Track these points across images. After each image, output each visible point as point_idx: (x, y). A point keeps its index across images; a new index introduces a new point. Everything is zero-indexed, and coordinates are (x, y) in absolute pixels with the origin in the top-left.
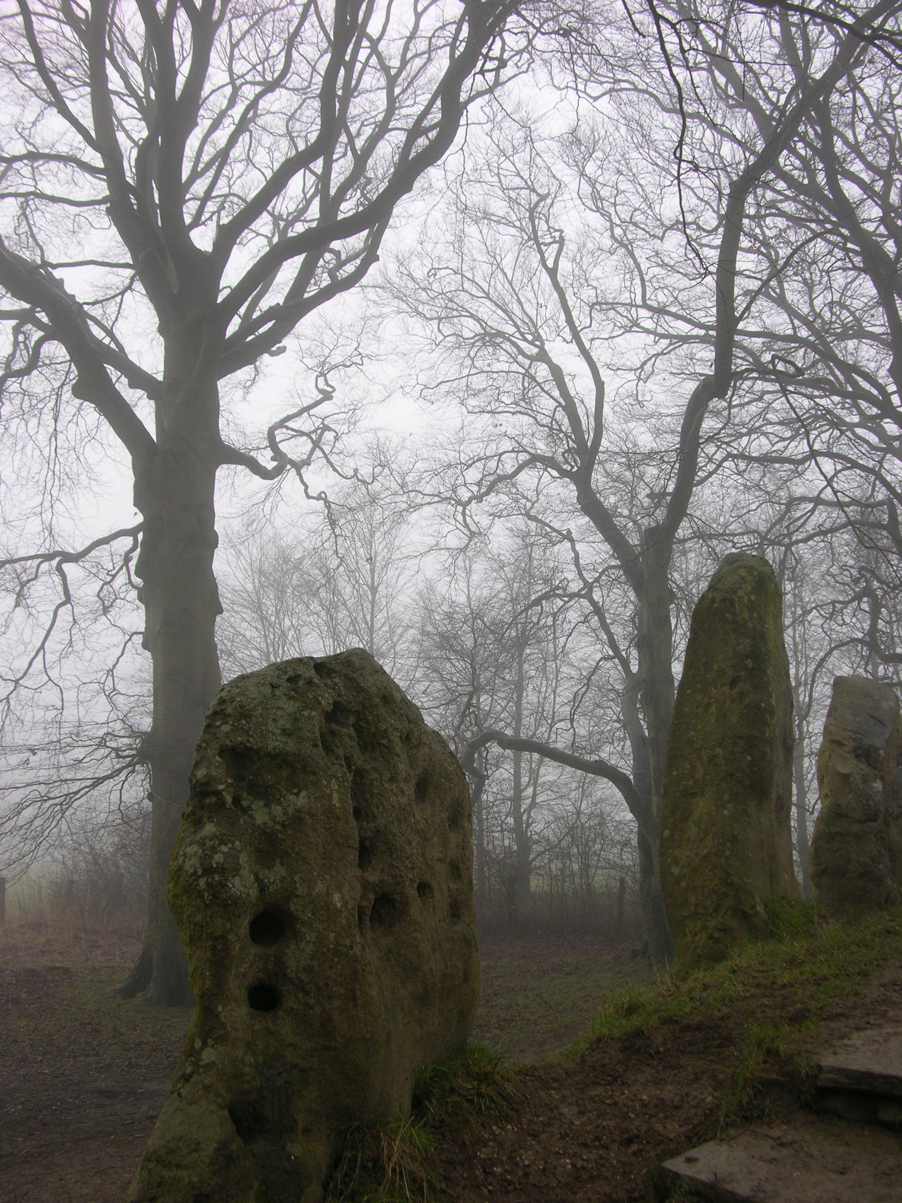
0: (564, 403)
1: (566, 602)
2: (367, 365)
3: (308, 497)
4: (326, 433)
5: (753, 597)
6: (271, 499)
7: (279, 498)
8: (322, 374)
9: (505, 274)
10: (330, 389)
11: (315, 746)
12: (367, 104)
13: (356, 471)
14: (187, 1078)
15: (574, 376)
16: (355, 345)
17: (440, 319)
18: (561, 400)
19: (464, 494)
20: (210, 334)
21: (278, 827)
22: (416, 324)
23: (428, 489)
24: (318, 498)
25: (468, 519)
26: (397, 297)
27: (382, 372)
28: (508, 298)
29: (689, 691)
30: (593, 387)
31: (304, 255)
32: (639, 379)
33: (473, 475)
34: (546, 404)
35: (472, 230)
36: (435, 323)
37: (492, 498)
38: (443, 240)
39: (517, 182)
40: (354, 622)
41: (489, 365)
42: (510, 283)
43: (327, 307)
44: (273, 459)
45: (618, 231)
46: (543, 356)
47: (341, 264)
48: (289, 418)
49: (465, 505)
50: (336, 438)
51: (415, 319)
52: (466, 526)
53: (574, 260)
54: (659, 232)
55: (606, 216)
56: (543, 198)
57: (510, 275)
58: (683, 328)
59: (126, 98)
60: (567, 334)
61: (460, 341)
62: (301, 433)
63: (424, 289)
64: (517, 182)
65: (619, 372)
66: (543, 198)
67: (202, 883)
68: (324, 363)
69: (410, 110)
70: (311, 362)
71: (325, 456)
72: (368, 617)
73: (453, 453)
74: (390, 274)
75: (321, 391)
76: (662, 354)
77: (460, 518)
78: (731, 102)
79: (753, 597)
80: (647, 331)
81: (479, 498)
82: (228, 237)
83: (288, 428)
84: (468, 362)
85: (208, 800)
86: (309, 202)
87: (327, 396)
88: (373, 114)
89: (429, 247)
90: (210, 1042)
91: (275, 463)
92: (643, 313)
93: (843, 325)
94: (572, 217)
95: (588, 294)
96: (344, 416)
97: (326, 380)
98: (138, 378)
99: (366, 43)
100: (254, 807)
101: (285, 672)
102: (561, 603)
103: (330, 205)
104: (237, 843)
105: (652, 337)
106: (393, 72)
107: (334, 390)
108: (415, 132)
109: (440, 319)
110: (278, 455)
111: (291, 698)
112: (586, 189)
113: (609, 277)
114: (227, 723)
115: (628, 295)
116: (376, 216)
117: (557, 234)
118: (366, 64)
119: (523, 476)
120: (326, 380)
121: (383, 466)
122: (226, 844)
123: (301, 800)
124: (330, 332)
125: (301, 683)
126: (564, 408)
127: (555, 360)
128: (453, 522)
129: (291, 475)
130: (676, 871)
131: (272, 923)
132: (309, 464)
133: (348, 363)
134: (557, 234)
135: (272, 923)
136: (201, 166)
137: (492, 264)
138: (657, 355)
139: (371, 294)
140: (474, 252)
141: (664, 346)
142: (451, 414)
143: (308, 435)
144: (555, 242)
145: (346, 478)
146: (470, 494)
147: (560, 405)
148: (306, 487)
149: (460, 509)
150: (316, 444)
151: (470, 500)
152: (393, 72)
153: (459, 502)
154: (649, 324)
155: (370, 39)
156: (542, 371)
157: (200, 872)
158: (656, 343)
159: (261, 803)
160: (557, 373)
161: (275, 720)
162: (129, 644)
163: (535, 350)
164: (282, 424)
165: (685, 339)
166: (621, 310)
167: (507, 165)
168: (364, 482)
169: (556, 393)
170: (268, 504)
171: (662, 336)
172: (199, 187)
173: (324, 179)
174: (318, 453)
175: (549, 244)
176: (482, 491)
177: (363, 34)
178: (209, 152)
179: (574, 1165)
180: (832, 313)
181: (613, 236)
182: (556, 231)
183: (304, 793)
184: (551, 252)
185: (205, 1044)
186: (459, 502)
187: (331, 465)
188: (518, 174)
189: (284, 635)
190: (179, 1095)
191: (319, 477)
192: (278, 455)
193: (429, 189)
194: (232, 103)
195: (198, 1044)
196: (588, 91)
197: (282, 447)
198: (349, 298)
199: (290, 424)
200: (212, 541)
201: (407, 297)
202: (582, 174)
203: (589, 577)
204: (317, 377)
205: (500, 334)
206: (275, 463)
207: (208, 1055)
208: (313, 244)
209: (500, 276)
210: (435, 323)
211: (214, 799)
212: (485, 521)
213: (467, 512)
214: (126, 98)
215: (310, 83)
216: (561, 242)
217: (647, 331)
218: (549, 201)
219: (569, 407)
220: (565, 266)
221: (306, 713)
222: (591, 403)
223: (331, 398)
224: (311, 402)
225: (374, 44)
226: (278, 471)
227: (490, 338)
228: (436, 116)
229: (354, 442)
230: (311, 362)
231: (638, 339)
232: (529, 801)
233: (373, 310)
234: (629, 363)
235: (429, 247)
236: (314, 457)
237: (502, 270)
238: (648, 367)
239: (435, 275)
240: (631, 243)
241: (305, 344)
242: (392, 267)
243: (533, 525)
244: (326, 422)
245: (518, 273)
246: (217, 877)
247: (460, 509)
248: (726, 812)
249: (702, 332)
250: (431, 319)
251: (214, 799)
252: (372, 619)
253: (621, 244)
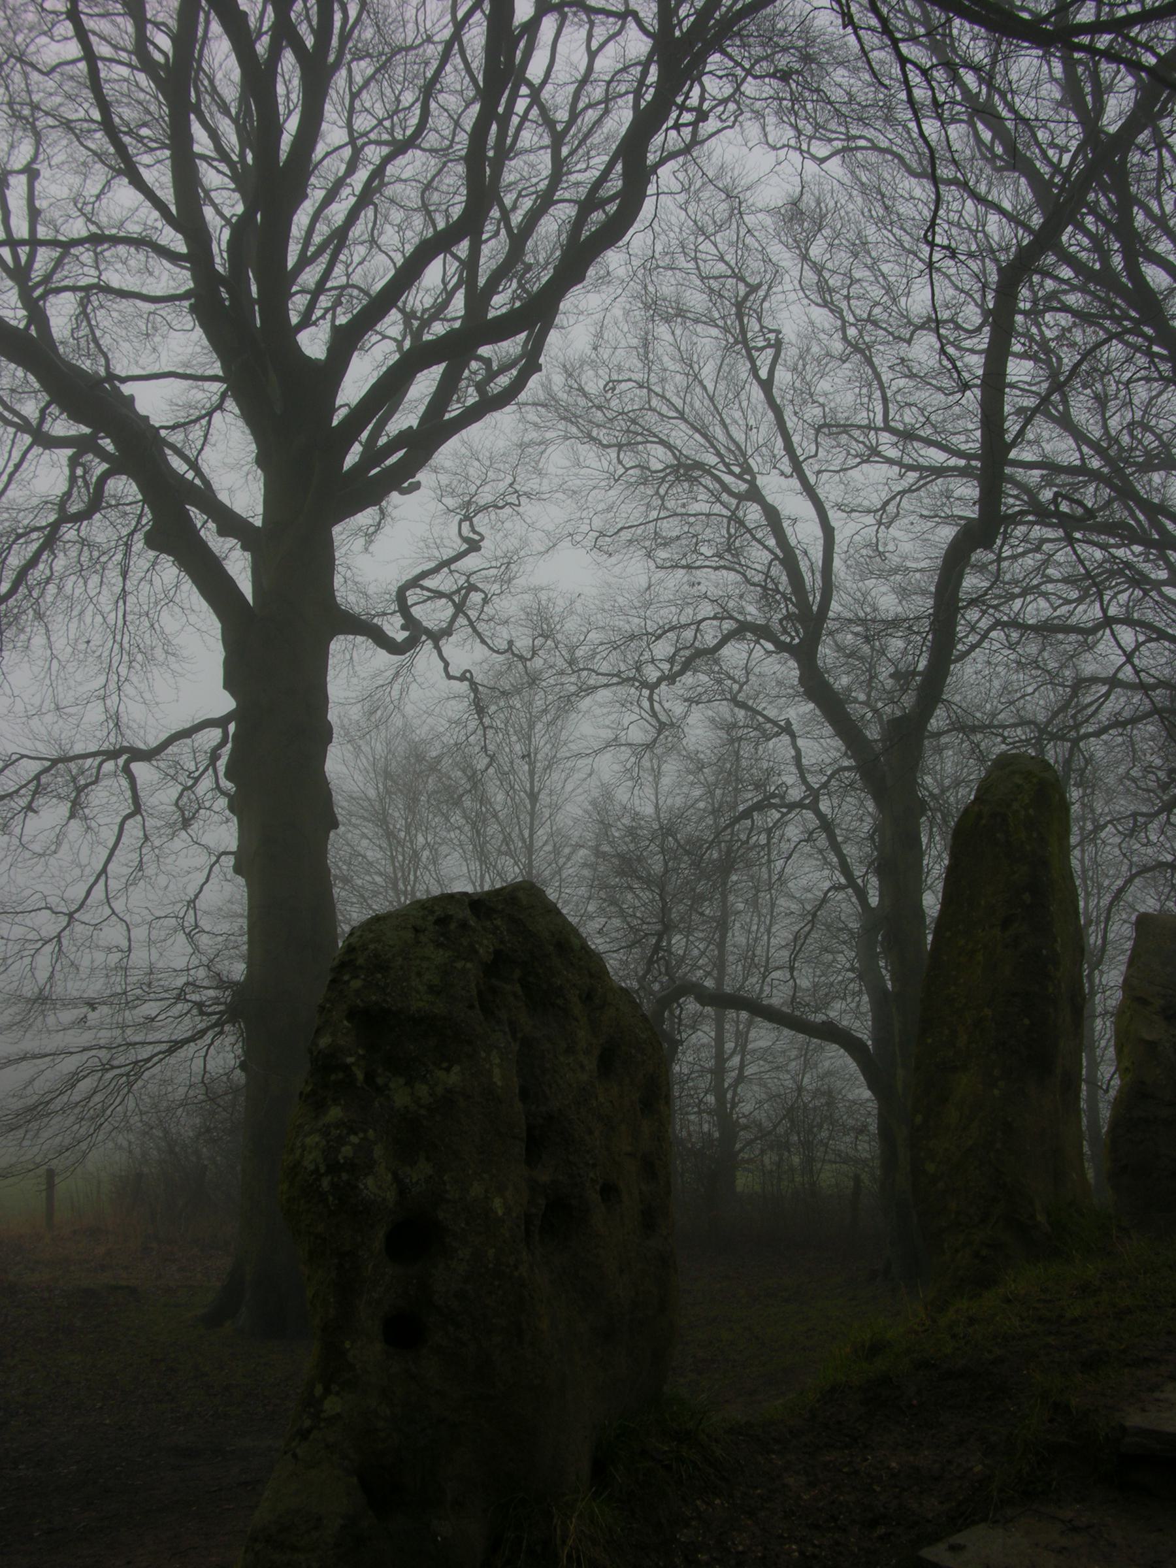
0: (781, 555)
1: (784, 815)
2: (526, 507)
3: (450, 677)
4: (473, 594)
5: (1031, 811)
6: (400, 680)
7: (410, 679)
8: (467, 518)
9: (704, 388)
10: (477, 537)
11: (471, 1007)
12: (528, 166)
13: (511, 643)
14: (304, 1435)
15: (795, 520)
16: (509, 479)
17: (620, 446)
18: (778, 551)
19: (652, 674)
20: (324, 472)
22: (588, 453)
23: (605, 667)
24: (462, 678)
25: (656, 705)
26: (564, 418)
27: (548, 515)
28: (708, 419)
29: (948, 934)
30: (820, 534)
31: (444, 365)
32: (880, 523)
33: (662, 649)
34: (758, 557)
35: (662, 330)
36: (613, 453)
37: (688, 679)
38: (623, 343)
39: (721, 268)
40: (507, 840)
41: (684, 506)
42: (712, 399)
43: (474, 432)
44: (403, 628)
45: (852, 332)
46: (754, 494)
47: (492, 376)
48: (424, 575)
49: (653, 687)
50: (486, 601)
51: (587, 446)
52: (654, 714)
53: (795, 369)
54: (905, 333)
55: (836, 311)
56: (754, 289)
57: (710, 387)
58: (937, 457)
59: (215, 163)
60: (786, 465)
61: (646, 475)
62: (439, 594)
63: (599, 408)
64: (721, 268)
65: (854, 515)
66: (754, 289)
67: (325, 1183)
68: (469, 503)
69: (583, 175)
70: (450, 502)
71: (471, 624)
72: (526, 833)
73: (636, 620)
74: (555, 388)
75: (466, 540)
76: (909, 490)
77: (646, 704)
78: (999, 163)
79: (1031, 811)
81: (671, 679)
82: (346, 342)
83: (423, 588)
84: (656, 502)
85: (333, 1077)
86: (450, 295)
87: (473, 546)
88: (534, 180)
89: (605, 353)
90: (335, 1388)
91: (406, 634)
92: (885, 437)
93: (1147, 453)
94: (792, 314)
95: (813, 413)
96: (494, 572)
97: (472, 525)
98: (230, 523)
99: (524, 90)
100: (392, 1085)
101: (432, 912)
102: (777, 815)
103: (478, 300)
104: (371, 1132)
105: (896, 469)
106: (559, 127)
107: (483, 538)
108: (588, 204)
109: (620, 446)
110: (411, 623)
111: (439, 945)
112: (810, 276)
113: (839, 389)
114: (357, 977)
115: (865, 414)
116: (537, 314)
117: (772, 336)
118: (524, 118)
119: (726, 651)
120: (472, 525)
121: (547, 637)
122: (356, 1134)
123: (453, 1077)
124: (476, 464)
125: (453, 926)
126: (782, 562)
127: (769, 499)
128: (637, 710)
129: (427, 648)
130: (931, 1168)
131: (415, 1234)
132: (450, 635)
133: (501, 504)
134: (772, 336)
135: (415, 1234)
136: (312, 249)
137: (687, 375)
138: (903, 493)
139: (531, 415)
140: (666, 359)
141: (911, 481)
142: (635, 570)
143: (449, 596)
144: (769, 346)
145: (497, 652)
146: (659, 674)
147: (776, 557)
148: (447, 665)
149: (646, 692)
150: (460, 609)
151: (660, 680)
152: (559, 127)
153: (645, 684)
154: (893, 453)
155: (529, 84)
156: (753, 513)
158: (902, 476)
159: (402, 1081)
160: (772, 516)
161: (419, 974)
162: (217, 868)
163: (744, 487)
164: (415, 582)
165: (940, 471)
166: (856, 433)
167: (706, 246)
168: (521, 658)
169: (772, 542)
170: (397, 687)
171: (910, 468)
172: (310, 277)
173: (471, 265)
174: (461, 620)
175: (762, 349)
176: (675, 669)
177: (521, 79)
178: (322, 231)
179: (802, 1553)
180: (1133, 437)
181: (845, 338)
182: (771, 331)
183: (456, 1068)
184: (764, 360)
185: (327, 1391)
186: (645, 684)
187: (479, 635)
188: (722, 259)
189: (416, 855)
190: (295, 1456)
191: (463, 652)
192: (411, 623)
193: (606, 278)
194: (352, 168)
195: (319, 1390)
196: (813, 150)
197: (416, 612)
198: (504, 419)
199: (426, 583)
200: (324, 734)
201: (578, 417)
202: (805, 258)
203: (815, 781)
204: (461, 521)
205: (699, 465)
206: (406, 634)
207: (332, 1405)
208: (455, 350)
209: (698, 390)
210: (613, 453)
211: (341, 1075)
212: (678, 709)
213: (656, 697)
214: (215, 163)
215: (452, 141)
216: (778, 345)
217: (890, 461)
218: (761, 293)
219: (788, 558)
220: (783, 377)
221: (459, 965)
222: (817, 554)
223: (478, 549)
224: (452, 553)
225: (536, 93)
226: (410, 644)
227: (685, 470)
228: (615, 184)
229: (507, 605)
230: (450, 502)
231: (878, 472)
232: (734, 1074)
233: (533, 435)
234: (866, 503)
235: (605, 353)
236: (456, 625)
237: (701, 382)
238: (891, 509)
239: (613, 389)
240: (869, 348)
241: (444, 479)
242: (558, 379)
243: (741, 713)
244: (472, 580)
245: (722, 386)
246: (345, 1176)
247: (646, 692)
248: (996, 1092)
249: (962, 462)
250: (609, 446)
251: (341, 1075)
252: (531, 836)
253: (857, 349)
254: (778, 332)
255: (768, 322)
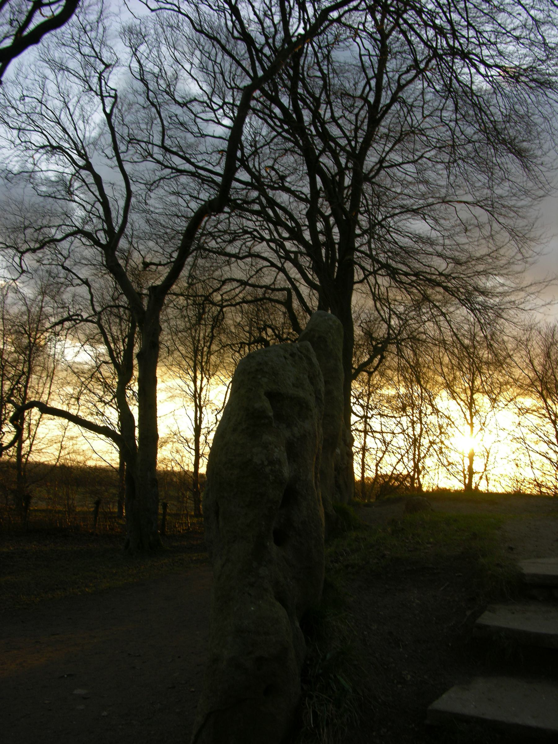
15: (113, 184)
17: (19, 129)
18: (99, 197)
21: (295, 440)
36: (15, 132)
42: (71, 116)
46: (88, 167)
49: (23, 253)
52: (21, 267)
55: (146, 85)
66: (107, 66)
67: (268, 469)
80: (158, 162)
81: (34, 251)
92: (156, 149)
105: (158, 166)
109: (19, 129)
117: (112, 93)
146: (28, 247)
147: (99, 201)
151: (27, 250)
157: (266, 463)
160: (98, 180)
166: (143, 145)
171: (167, 167)
175: (106, 97)
205: (60, 148)
216: (116, 97)
217: (158, 162)
239: (24, 100)
246: (277, 466)
249: (192, 169)
254: (116, 90)
255: (111, 84)
